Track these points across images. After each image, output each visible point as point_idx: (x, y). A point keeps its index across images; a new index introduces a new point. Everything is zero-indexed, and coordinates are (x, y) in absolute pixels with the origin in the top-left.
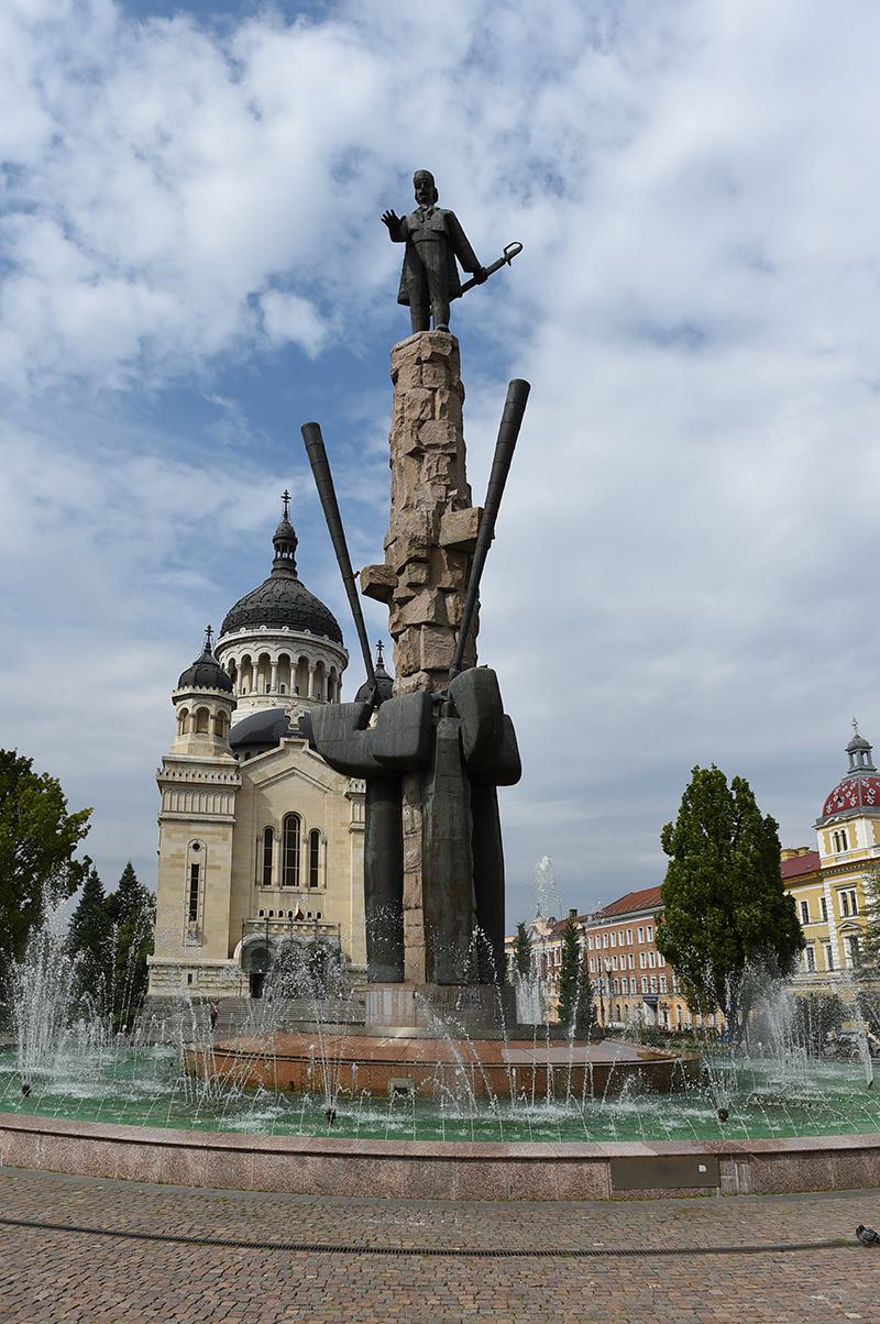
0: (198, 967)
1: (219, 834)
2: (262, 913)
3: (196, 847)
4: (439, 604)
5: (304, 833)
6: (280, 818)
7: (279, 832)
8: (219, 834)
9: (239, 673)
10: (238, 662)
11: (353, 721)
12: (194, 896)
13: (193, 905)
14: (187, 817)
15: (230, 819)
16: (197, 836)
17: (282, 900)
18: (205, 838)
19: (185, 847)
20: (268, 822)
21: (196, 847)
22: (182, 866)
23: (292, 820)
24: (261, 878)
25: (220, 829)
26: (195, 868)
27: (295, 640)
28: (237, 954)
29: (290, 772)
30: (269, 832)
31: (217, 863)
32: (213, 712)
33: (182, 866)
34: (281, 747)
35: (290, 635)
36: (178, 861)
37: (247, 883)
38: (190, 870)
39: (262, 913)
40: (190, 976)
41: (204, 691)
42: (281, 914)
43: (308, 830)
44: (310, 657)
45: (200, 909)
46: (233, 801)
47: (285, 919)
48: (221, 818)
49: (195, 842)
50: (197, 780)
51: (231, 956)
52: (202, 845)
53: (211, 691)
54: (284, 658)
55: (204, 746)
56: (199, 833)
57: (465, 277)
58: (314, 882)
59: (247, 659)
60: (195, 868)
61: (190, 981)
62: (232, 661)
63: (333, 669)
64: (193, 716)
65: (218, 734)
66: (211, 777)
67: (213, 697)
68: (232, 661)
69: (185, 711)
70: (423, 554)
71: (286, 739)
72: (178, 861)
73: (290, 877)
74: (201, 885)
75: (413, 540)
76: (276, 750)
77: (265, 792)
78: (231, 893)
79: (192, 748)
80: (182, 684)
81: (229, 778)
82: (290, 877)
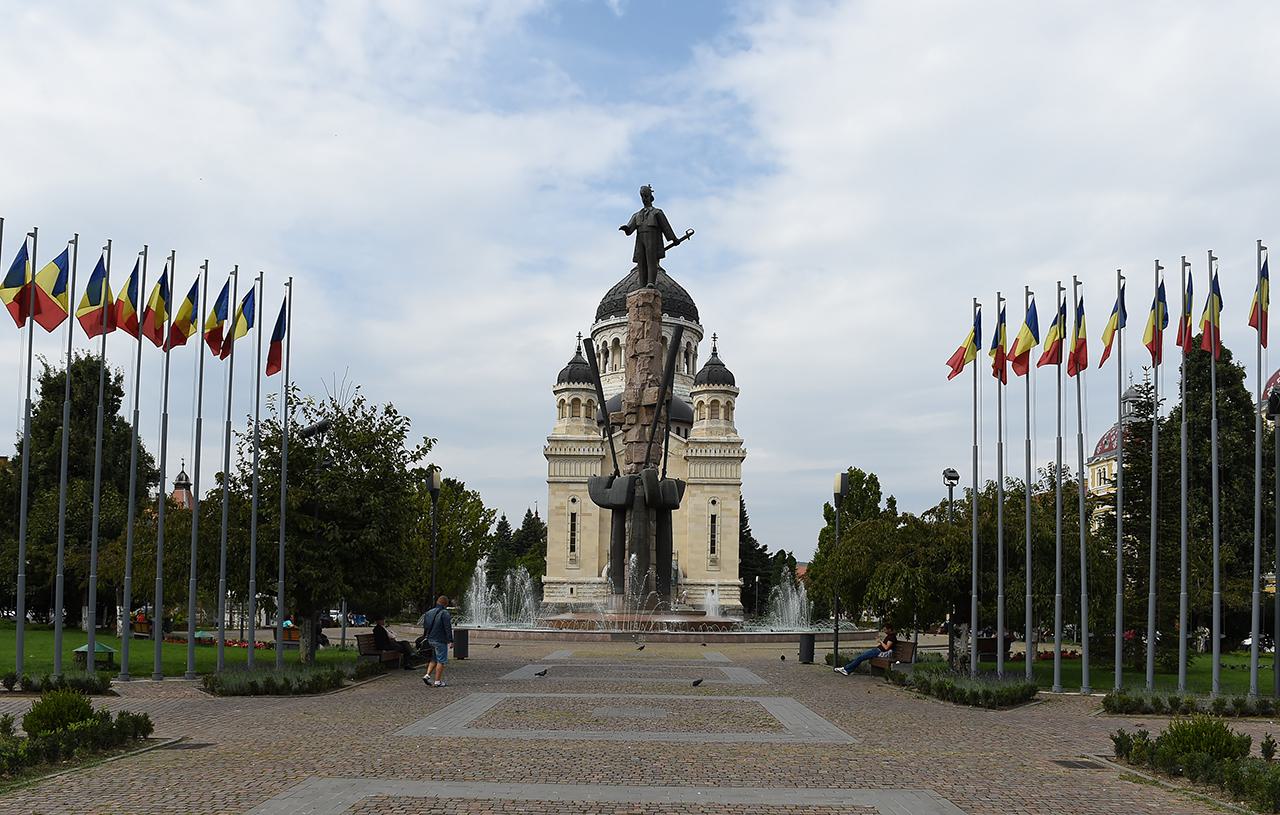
3: (574, 501)
4: (641, 433)
9: (610, 353)
10: (610, 344)
11: (605, 485)
12: (573, 535)
13: (573, 541)
18: (580, 494)
19: (565, 500)
21: (574, 501)
22: (565, 514)
26: (573, 516)
28: (604, 573)
31: (589, 512)
32: (583, 401)
33: (565, 514)
40: (572, 589)
41: (576, 386)
45: (577, 544)
46: (599, 465)
50: (572, 453)
51: (600, 575)
52: (578, 499)
53: (585, 386)
55: (576, 427)
56: (576, 490)
57: (666, 243)
59: (616, 341)
60: (573, 516)
61: (572, 592)
62: (605, 343)
63: (689, 344)
65: (588, 417)
66: (584, 450)
67: (583, 389)
68: (605, 343)
69: (563, 401)
70: (634, 411)
74: (578, 527)
75: (629, 404)
79: (568, 430)
80: (560, 381)
81: (596, 450)
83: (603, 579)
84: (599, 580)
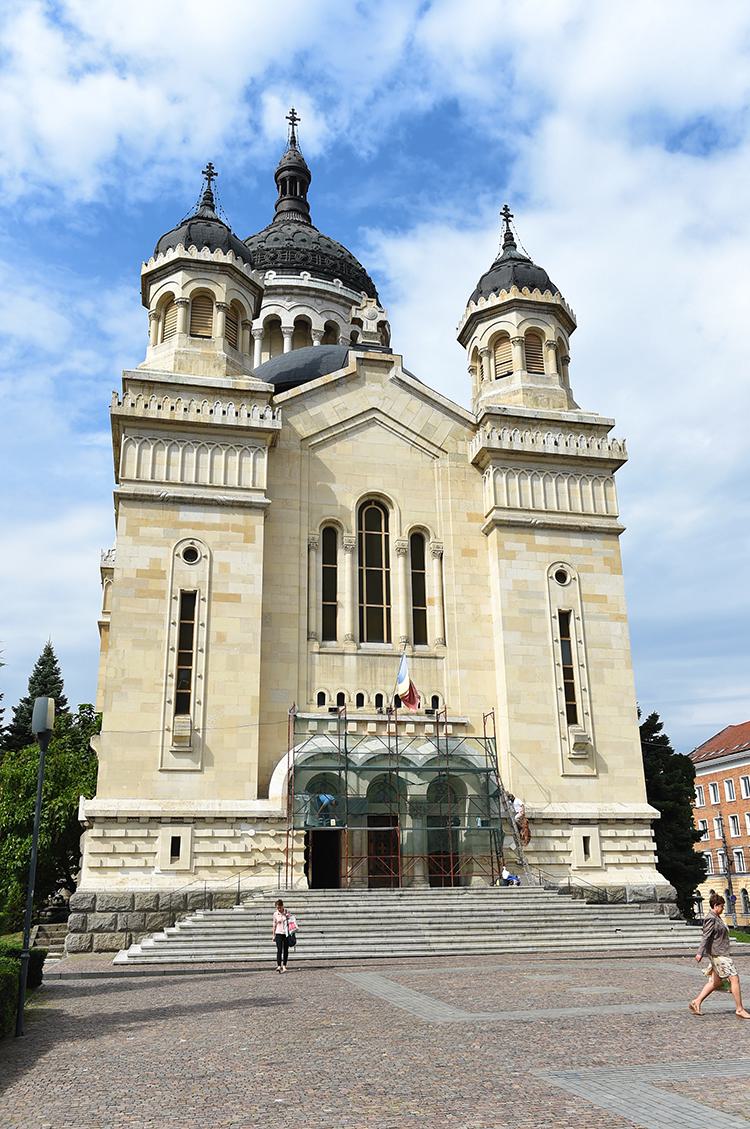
0: (198, 821)
1: (236, 528)
2: (321, 698)
3: (191, 555)
5: (397, 535)
6: (352, 505)
7: (350, 533)
8: (236, 528)
12: (185, 659)
13: (184, 679)
14: (171, 492)
15: (259, 498)
16: (190, 533)
17: (361, 671)
18: (211, 537)
20: (329, 513)
21: (191, 555)
23: (374, 510)
24: (317, 626)
25: (237, 518)
26: (188, 600)
27: (320, 294)
29: (369, 418)
30: (331, 535)
31: (233, 588)
33: (161, 595)
34: (352, 367)
35: (313, 285)
36: (154, 585)
37: (291, 636)
38: (177, 604)
39: (321, 698)
40: (176, 842)
41: (206, 255)
42: (360, 699)
43: (406, 529)
44: (340, 323)
45: (197, 690)
46: (263, 462)
47: (369, 711)
48: (240, 496)
49: (187, 544)
51: (263, 794)
52: (202, 551)
54: (302, 324)
56: (197, 526)
58: (419, 634)
60: (188, 600)
64: (184, 303)
71: (361, 354)
72: (154, 585)
73: (374, 626)
74: (199, 636)
76: (341, 373)
77: (323, 454)
78: (264, 658)
79: (181, 362)
82: (374, 626)
83: (276, 803)
84: (259, 807)
